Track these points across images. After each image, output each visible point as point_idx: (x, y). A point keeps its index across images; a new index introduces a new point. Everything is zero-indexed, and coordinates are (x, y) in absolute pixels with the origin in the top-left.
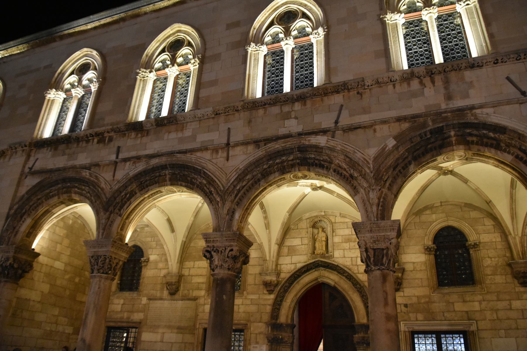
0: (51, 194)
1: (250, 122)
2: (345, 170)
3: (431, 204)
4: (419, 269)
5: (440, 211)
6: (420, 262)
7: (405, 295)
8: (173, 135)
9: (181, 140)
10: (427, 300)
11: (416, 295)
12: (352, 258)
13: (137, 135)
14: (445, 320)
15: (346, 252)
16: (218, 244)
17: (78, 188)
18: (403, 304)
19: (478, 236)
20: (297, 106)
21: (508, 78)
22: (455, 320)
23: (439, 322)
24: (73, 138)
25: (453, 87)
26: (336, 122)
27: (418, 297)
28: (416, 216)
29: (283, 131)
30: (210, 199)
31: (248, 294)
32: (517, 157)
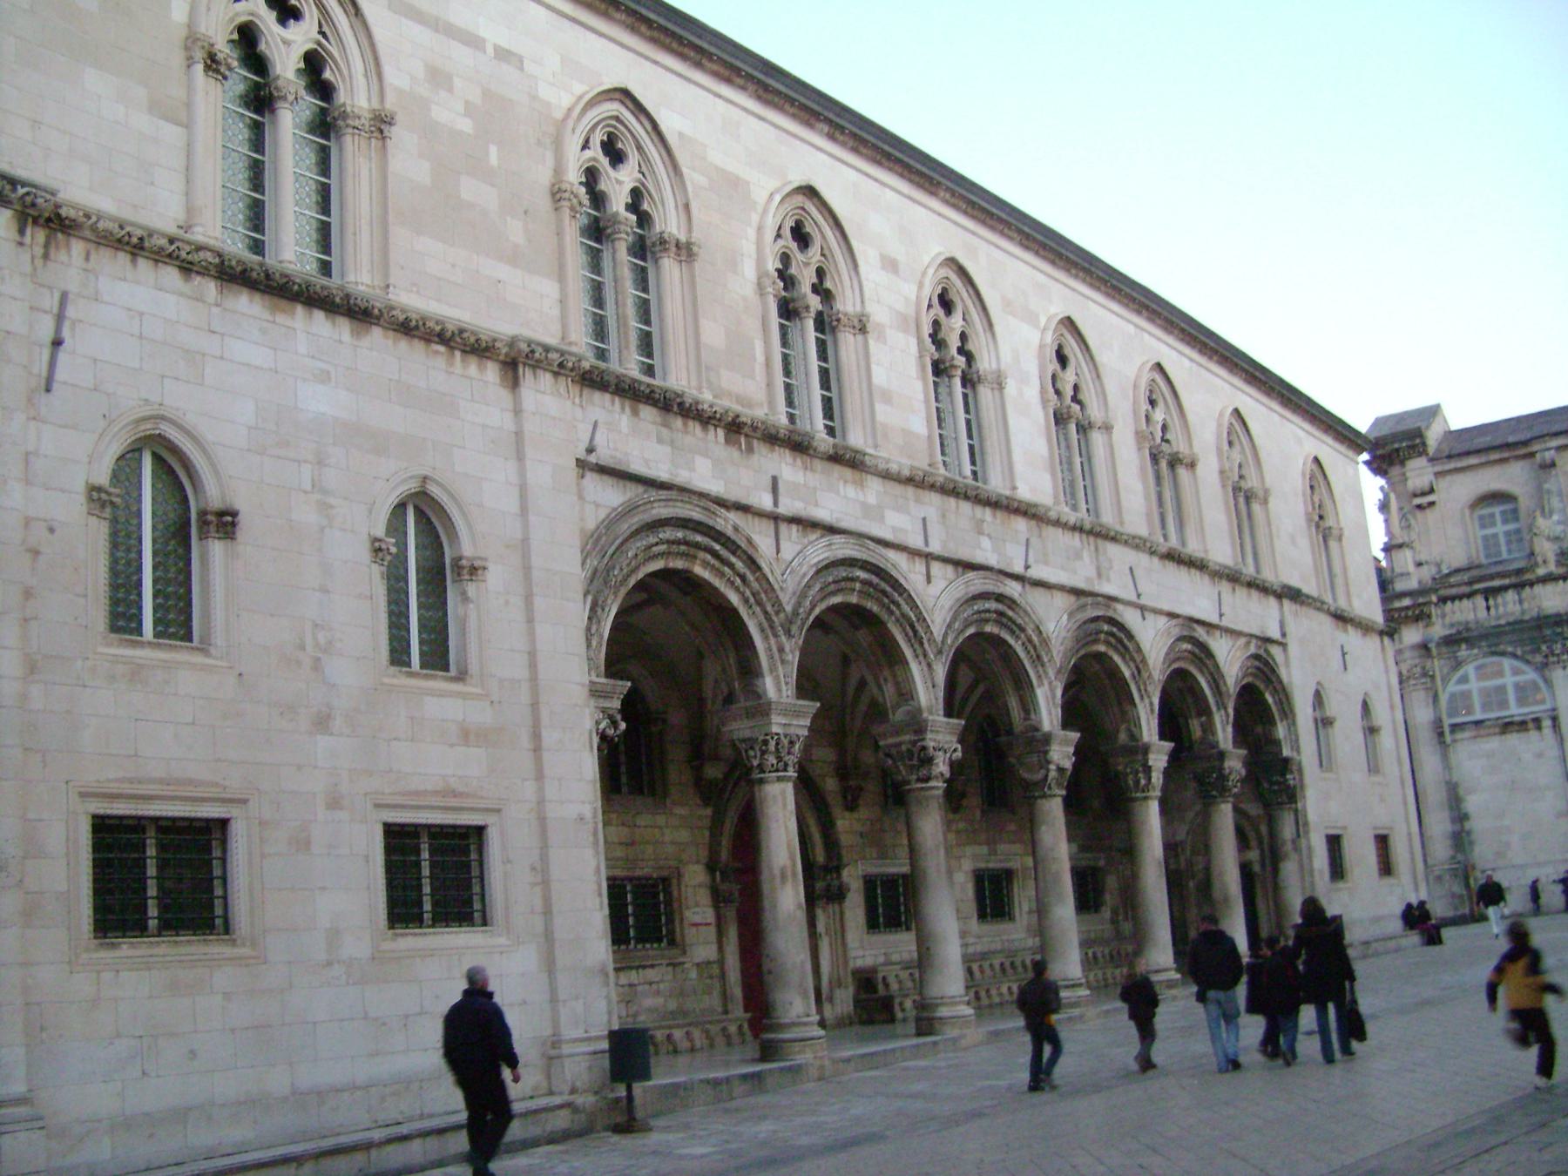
0: (654, 549)
1: (944, 516)
2: (1035, 647)
8: (851, 491)
9: (866, 508)
13: (795, 460)
16: (940, 737)
17: (715, 555)
20: (987, 514)
21: (1131, 569)
24: (681, 404)
25: (1101, 558)
26: (1027, 567)
29: (979, 557)
30: (915, 651)
31: (674, 803)
32: (1133, 675)
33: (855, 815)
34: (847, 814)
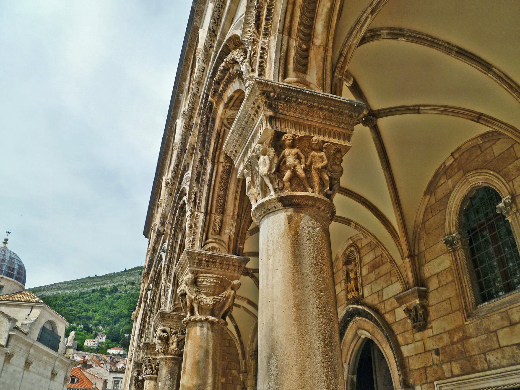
3: (441, 166)
4: (445, 283)
5: (456, 170)
6: (445, 269)
7: (435, 333)
10: (461, 335)
11: (447, 330)
12: (378, 292)
14: (490, 369)
15: (373, 286)
18: (433, 349)
19: (512, 186)
22: (503, 367)
23: (481, 374)
27: (450, 333)
28: (431, 195)
33: (428, 332)
34: (418, 336)
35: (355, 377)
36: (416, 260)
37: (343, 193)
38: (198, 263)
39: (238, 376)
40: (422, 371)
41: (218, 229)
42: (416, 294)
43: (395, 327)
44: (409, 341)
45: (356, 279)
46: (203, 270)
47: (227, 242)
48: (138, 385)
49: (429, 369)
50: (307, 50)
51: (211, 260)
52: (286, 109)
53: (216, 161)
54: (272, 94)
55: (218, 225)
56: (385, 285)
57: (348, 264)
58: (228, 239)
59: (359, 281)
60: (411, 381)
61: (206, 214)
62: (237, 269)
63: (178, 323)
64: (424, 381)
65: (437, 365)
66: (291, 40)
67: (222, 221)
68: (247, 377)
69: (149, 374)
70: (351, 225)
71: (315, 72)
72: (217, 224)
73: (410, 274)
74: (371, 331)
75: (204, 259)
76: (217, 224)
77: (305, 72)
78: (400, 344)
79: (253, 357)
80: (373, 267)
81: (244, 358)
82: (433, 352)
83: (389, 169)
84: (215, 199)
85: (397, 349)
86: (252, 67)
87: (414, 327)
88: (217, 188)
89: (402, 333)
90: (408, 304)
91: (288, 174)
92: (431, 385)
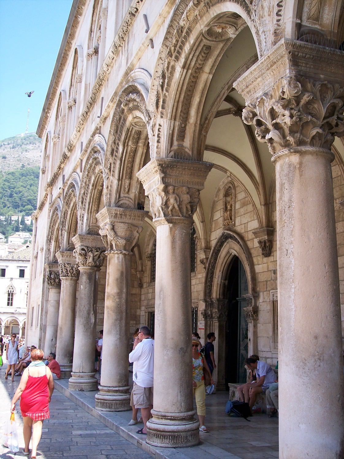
12: (245, 224)
34: (265, 259)
35: (227, 282)
36: (270, 207)
37: (221, 153)
38: (114, 216)
39: (135, 274)
40: (265, 283)
41: (127, 190)
42: (266, 233)
43: (252, 251)
44: (260, 263)
45: (231, 210)
46: (118, 220)
47: (133, 199)
48: (51, 282)
49: (268, 282)
50: (185, 127)
51: (123, 214)
52: (171, 171)
53: (126, 145)
54: (164, 165)
55: (127, 187)
56: (249, 220)
57: (227, 197)
58: (134, 197)
59: (233, 213)
60: (258, 289)
61: (119, 180)
62: (140, 219)
63: (93, 243)
64: (265, 290)
65: (273, 280)
66: (176, 122)
67: (130, 184)
68: (143, 275)
69: (65, 276)
70: (227, 174)
71: (189, 139)
72: (126, 187)
73: (264, 217)
74: (238, 251)
75: (118, 213)
76: (126, 187)
77: (183, 140)
78: (255, 264)
79: (148, 259)
80: (244, 204)
81: (141, 258)
82: (272, 272)
83: (254, 142)
84: (125, 169)
85: (252, 265)
86: (153, 133)
87: (263, 254)
88: (126, 162)
89: (256, 256)
90: (261, 238)
91: (170, 208)
92: (268, 292)
